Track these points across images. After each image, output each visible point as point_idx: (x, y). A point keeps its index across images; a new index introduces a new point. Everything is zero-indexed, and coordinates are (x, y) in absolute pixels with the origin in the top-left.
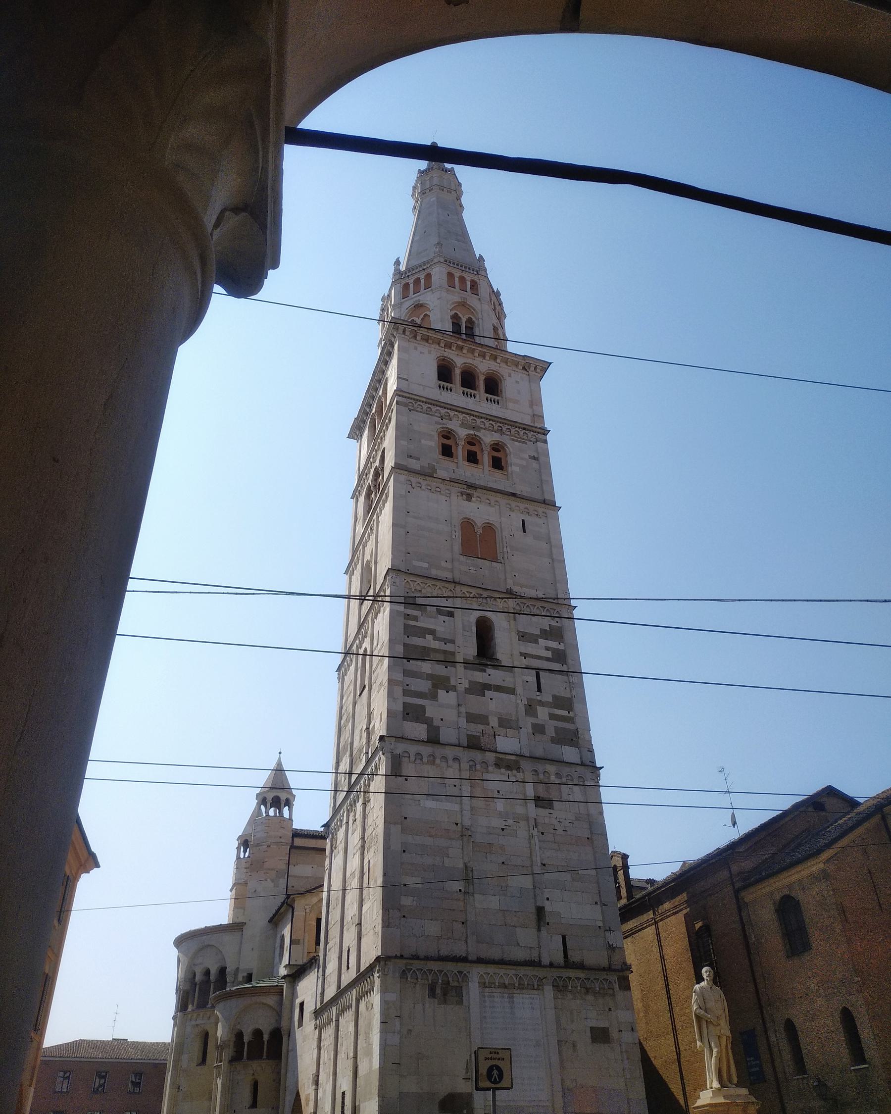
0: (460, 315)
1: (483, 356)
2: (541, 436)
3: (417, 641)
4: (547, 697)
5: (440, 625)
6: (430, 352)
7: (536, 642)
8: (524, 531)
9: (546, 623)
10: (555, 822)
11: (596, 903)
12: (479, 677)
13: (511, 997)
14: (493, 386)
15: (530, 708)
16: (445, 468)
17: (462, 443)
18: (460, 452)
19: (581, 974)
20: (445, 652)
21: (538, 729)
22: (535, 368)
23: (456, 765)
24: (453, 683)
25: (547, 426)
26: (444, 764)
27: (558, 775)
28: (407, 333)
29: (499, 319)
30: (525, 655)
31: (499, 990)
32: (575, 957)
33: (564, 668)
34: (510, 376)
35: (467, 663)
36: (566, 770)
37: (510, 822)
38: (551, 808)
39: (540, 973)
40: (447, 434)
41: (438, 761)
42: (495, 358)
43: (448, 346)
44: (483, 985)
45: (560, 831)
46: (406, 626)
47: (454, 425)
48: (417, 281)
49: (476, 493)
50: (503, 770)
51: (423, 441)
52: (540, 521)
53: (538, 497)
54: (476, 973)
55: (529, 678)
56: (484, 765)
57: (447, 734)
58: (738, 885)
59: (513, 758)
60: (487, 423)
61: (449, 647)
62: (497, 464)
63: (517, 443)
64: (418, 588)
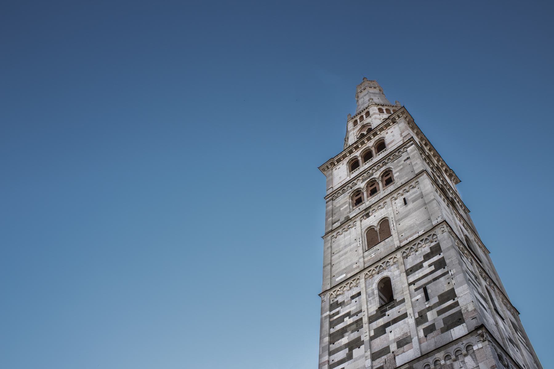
1: (369, 139)
4: (434, 300)
12: (381, 322)
14: (381, 146)
15: (421, 319)
20: (357, 322)
24: (362, 340)
27: (447, 357)
28: (329, 167)
30: (413, 283)
35: (371, 319)
36: (452, 350)
42: (375, 134)
43: (351, 152)
49: (371, 210)
55: (419, 297)
60: (376, 168)
64: (338, 293)
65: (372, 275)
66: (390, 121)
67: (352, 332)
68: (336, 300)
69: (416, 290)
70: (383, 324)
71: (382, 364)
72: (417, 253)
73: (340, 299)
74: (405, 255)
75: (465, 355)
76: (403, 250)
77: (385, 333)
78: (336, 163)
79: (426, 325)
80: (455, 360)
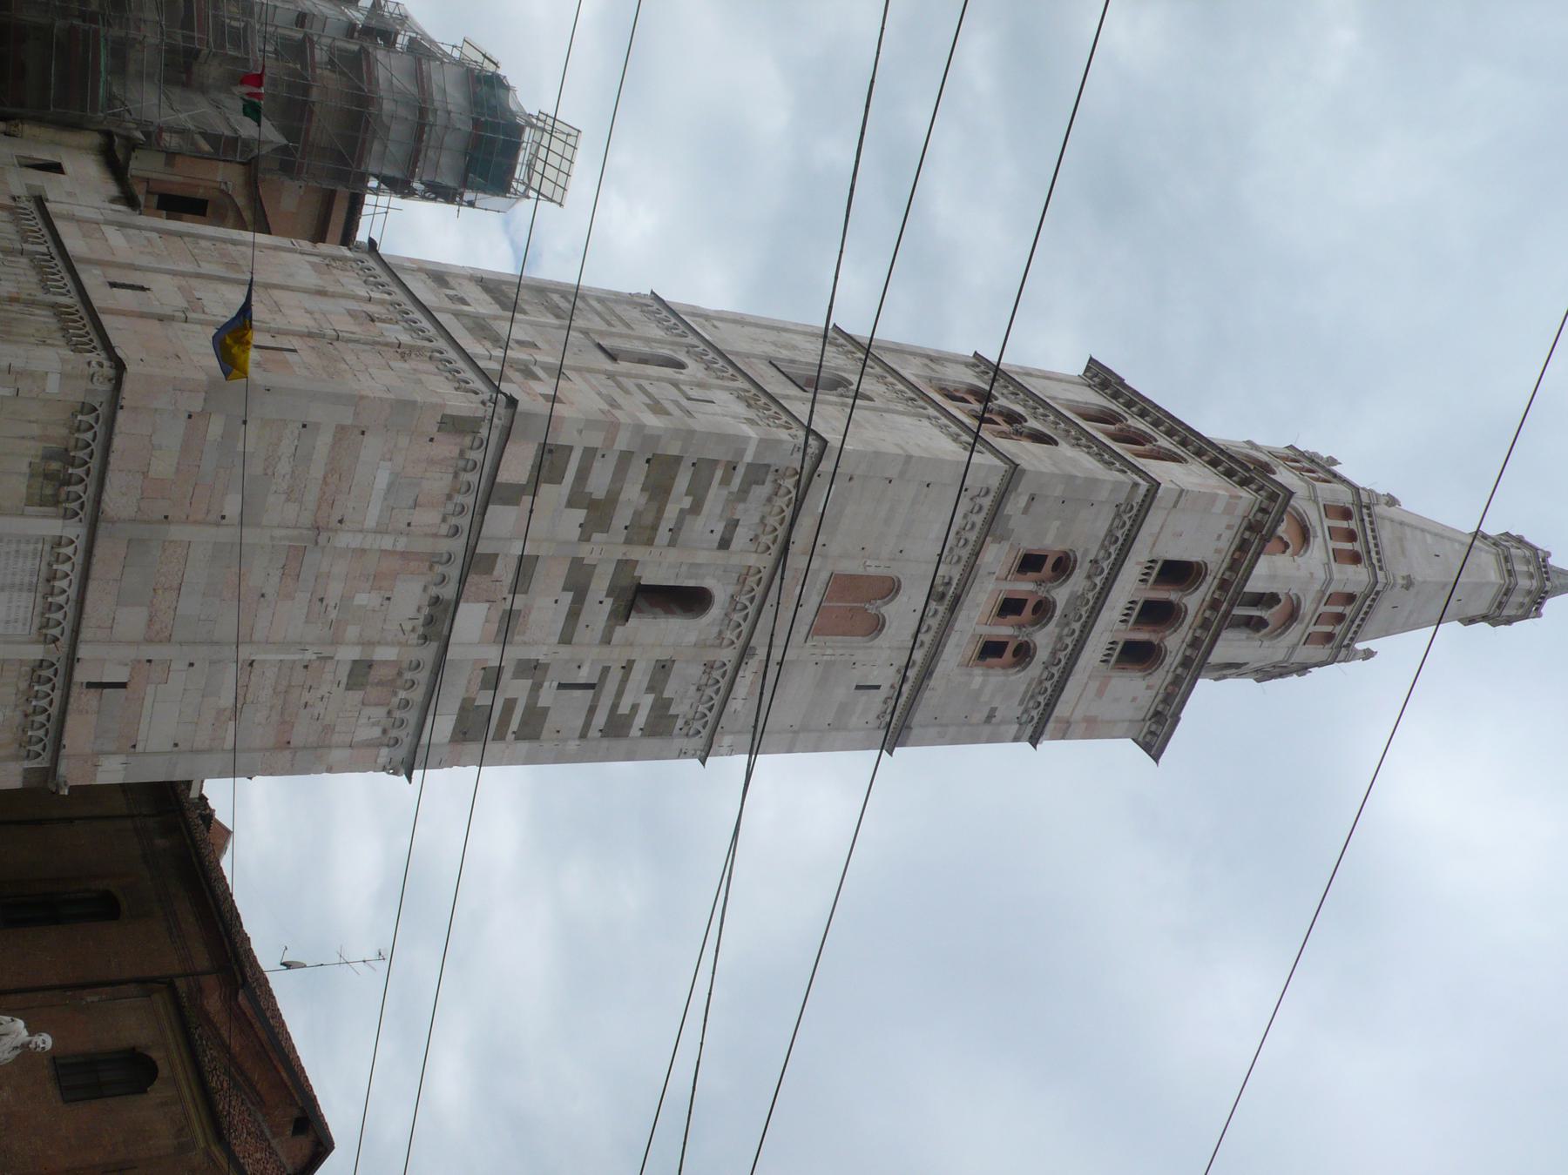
0: (1277, 608)
1: (1195, 643)
2: (1029, 730)
3: (682, 481)
4: (547, 697)
5: (709, 522)
6: (1217, 551)
7: (650, 689)
8: (858, 687)
9: (680, 708)
10: (324, 690)
11: (176, 745)
12: (599, 586)
13: (32, 588)
14: (1137, 655)
15: (533, 669)
16: (997, 557)
17: (1042, 593)
18: (1024, 587)
19: (54, 710)
20: (655, 528)
21: (493, 678)
22: (1154, 735)
23: (444, 529)
24: (597, 537)
25: (1046, 745)
26: (450, 507)
27: (406, 704)
28: (1260, 515)
29: (1257, 671)
30: (628, 668)
31: (44, 567)
32: (82, 700)
33: (594, 733)
34: (1149, 687)
36: (412, 716)
37: (333, 615)
38: (349, 688)
39: (64, 641)
40: (1064, 566)
41: (459, 499)
42: (1186, 662)
43: (1224, 585)
44: (58, 542)
45: (306, 696)
46: (715, 462)
47: (1077, 582)
48: (1351, 536)
50: (426, 611)
51: (1057, 523)
52: (872, 717)
53: (919, 717)
54: (75, 530)
56: (439, 578)
57: (502, 519)
58: (181, 984)
59: (445, 632)
61: (663, 535)
62: (991, 650)
63: (1023, 688)
65: (742, 580)
66: (1169, 712)
67: (637, 514)
68: (770, 478)
69: (606, 670)
70: (593, 586)
71: (495, 573)
72: (694, 688)
73: (761, 492)
74: (717, 664)
75: (384, 731)
76: (729, 667)
77: (565, 589)
78: (1247, 535)
79: (506, 676)
80: (389, 713)
